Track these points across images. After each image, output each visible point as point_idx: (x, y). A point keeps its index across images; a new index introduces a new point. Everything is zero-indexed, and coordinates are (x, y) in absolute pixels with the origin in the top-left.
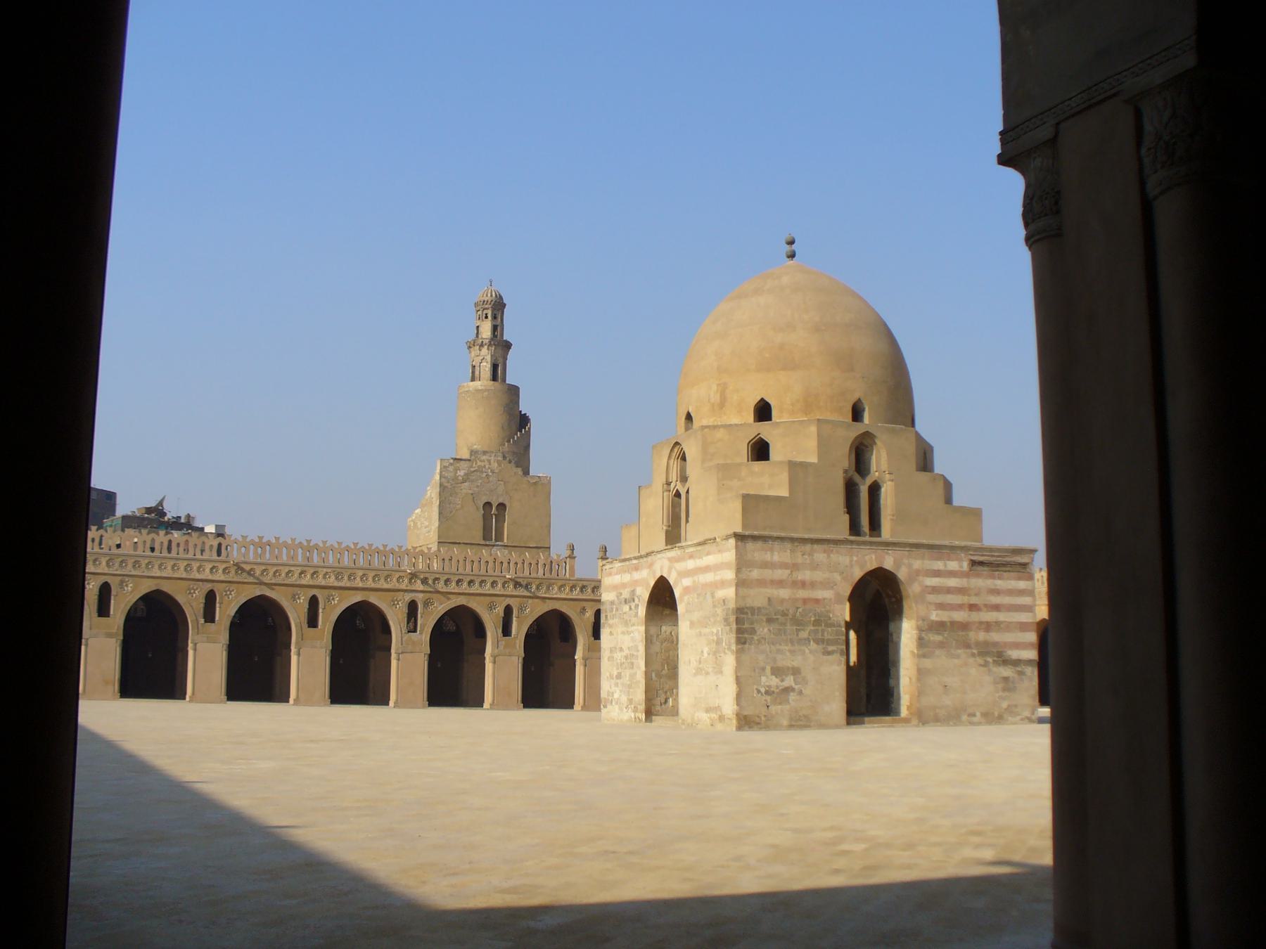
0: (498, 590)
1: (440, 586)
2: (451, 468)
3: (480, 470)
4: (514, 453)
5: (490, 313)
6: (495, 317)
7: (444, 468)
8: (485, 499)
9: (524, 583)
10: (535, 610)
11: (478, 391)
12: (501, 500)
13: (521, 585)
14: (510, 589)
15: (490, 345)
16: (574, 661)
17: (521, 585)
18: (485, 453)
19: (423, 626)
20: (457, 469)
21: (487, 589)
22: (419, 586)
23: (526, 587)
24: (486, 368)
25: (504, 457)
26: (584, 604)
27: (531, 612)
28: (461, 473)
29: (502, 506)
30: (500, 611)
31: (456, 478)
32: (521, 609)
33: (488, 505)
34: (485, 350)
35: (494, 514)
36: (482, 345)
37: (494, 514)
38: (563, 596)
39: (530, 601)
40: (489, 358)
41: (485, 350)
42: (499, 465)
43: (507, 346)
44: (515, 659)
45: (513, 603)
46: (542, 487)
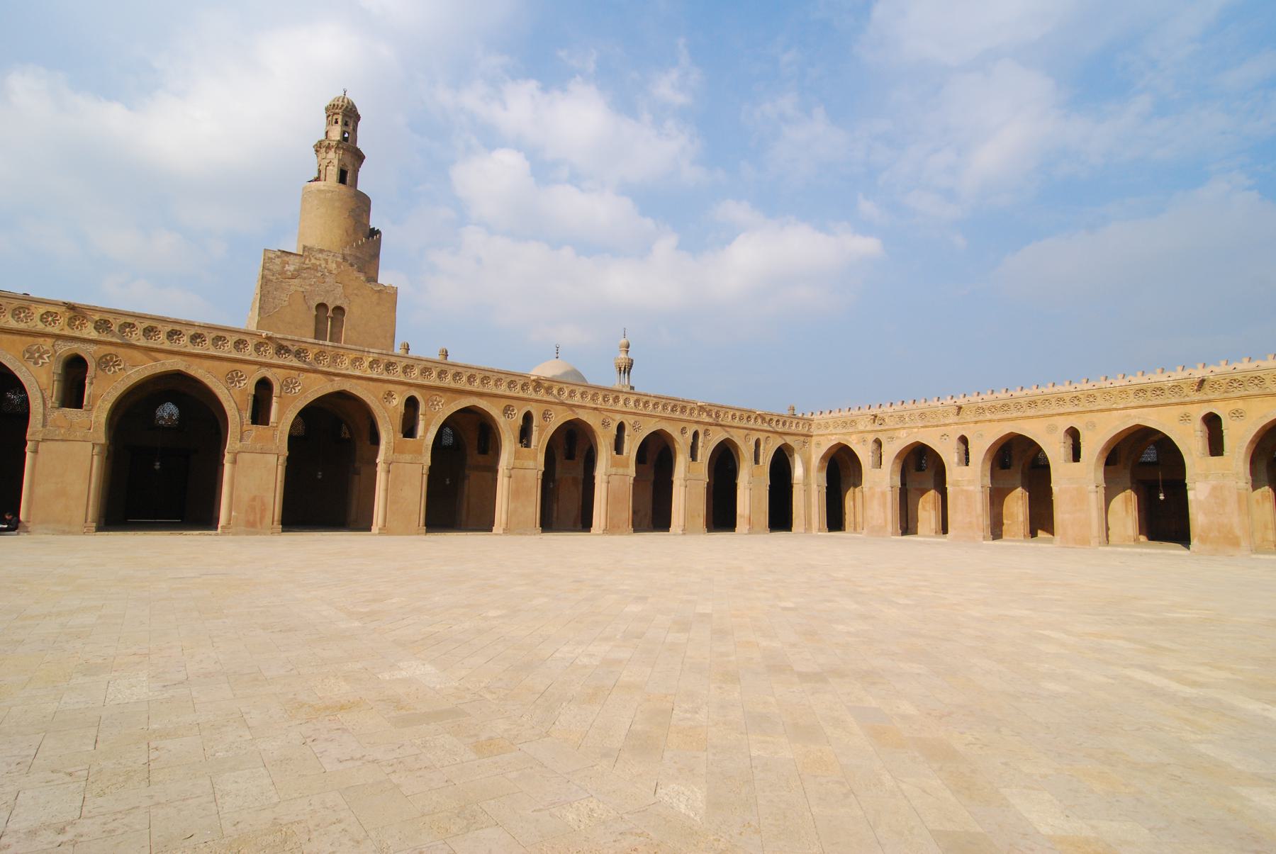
0: (249, 353)
1: (137, 338)
2: (278, 261)
3: (315, 268)
4: (357, 258)
5: (340, 118)
6: (346, 124)
7: (268, 260)
8: (319, 300)
9: (295, 349)
10: (314, 388)
11: (320, 191)
12: (338, 303)
13: (288, 351)
14: (270, 356)
15: (337, 148)
16: (376, 465)
17: (288, 351)
18: (321, 251)
19: (94, 398)
20: (285, 263)
21: (228, 350)
22: (90, 332)
23: (298, 354)
24: (333, 172)
25: (344, 259)
26: (391, 387)
27: (304, 391)
28: (292, 268)
29: (339, 310)
30: (249, 385)
31: (283, 273)
32: (288, 384)
33: (322, 306)
34: (331, 155)
35: (329, 318)
36: (328, 147)
37: (329, 318)
38: (358, 373)
39: (303, 376)
40: (336, 162)
41: (331, 155)
42: (338, 265)
43: (359, 157)
44: (273, 459)
45: (274, 376)
46: (389, 297)
